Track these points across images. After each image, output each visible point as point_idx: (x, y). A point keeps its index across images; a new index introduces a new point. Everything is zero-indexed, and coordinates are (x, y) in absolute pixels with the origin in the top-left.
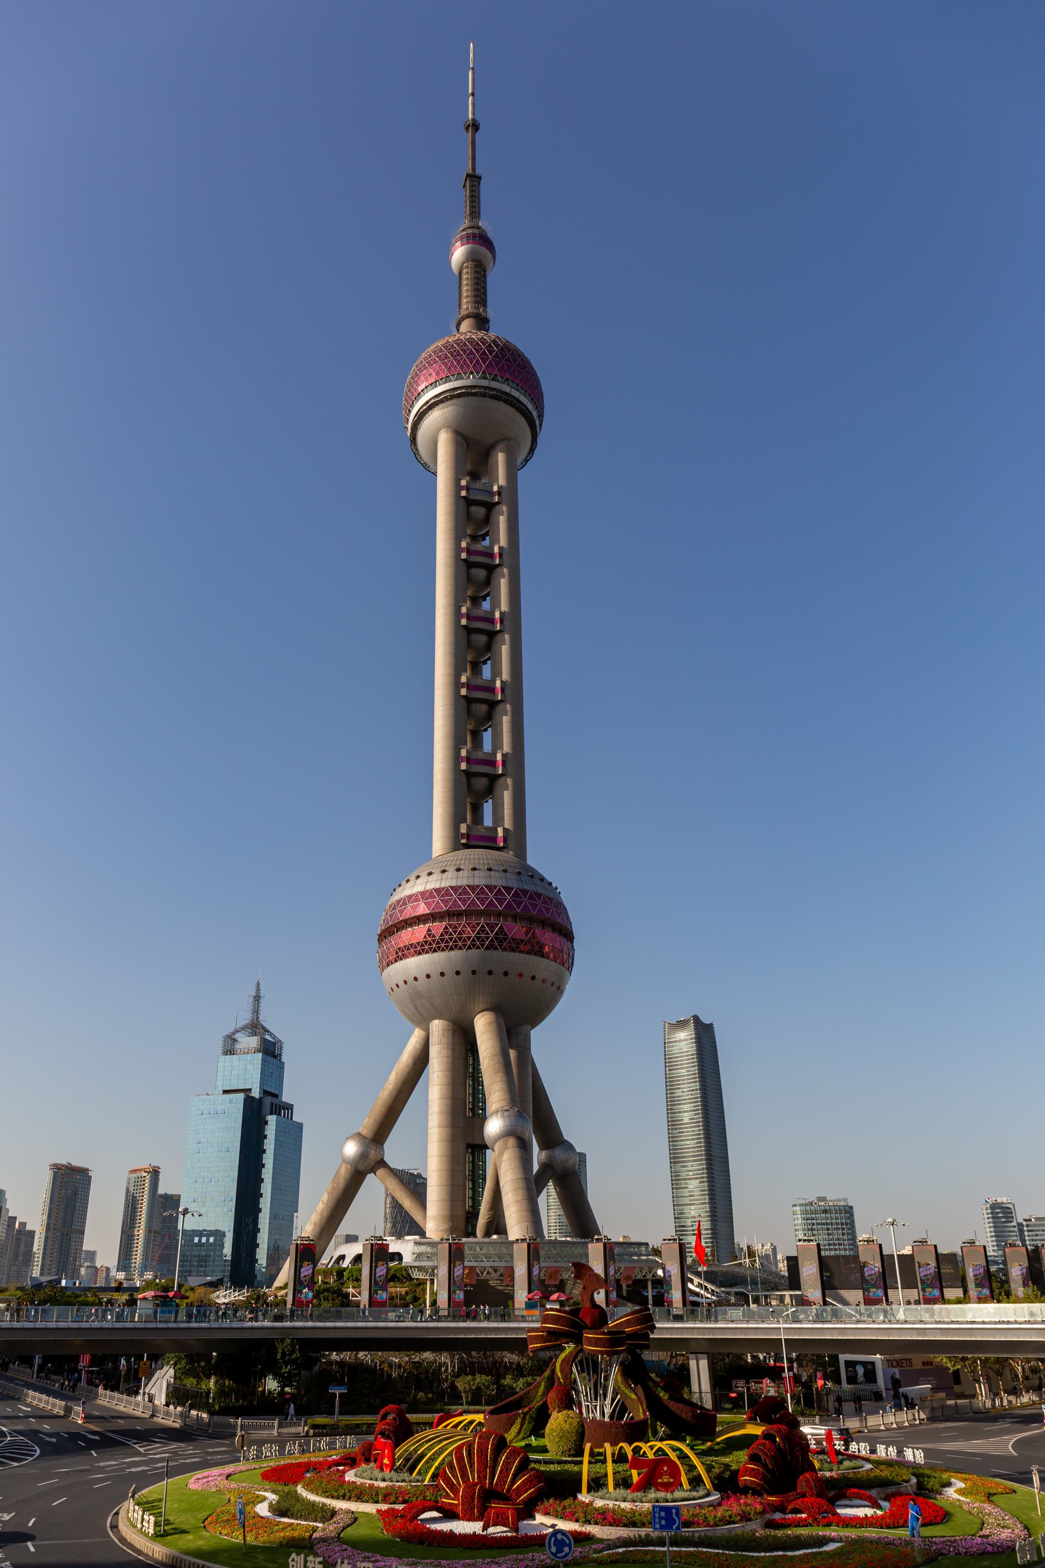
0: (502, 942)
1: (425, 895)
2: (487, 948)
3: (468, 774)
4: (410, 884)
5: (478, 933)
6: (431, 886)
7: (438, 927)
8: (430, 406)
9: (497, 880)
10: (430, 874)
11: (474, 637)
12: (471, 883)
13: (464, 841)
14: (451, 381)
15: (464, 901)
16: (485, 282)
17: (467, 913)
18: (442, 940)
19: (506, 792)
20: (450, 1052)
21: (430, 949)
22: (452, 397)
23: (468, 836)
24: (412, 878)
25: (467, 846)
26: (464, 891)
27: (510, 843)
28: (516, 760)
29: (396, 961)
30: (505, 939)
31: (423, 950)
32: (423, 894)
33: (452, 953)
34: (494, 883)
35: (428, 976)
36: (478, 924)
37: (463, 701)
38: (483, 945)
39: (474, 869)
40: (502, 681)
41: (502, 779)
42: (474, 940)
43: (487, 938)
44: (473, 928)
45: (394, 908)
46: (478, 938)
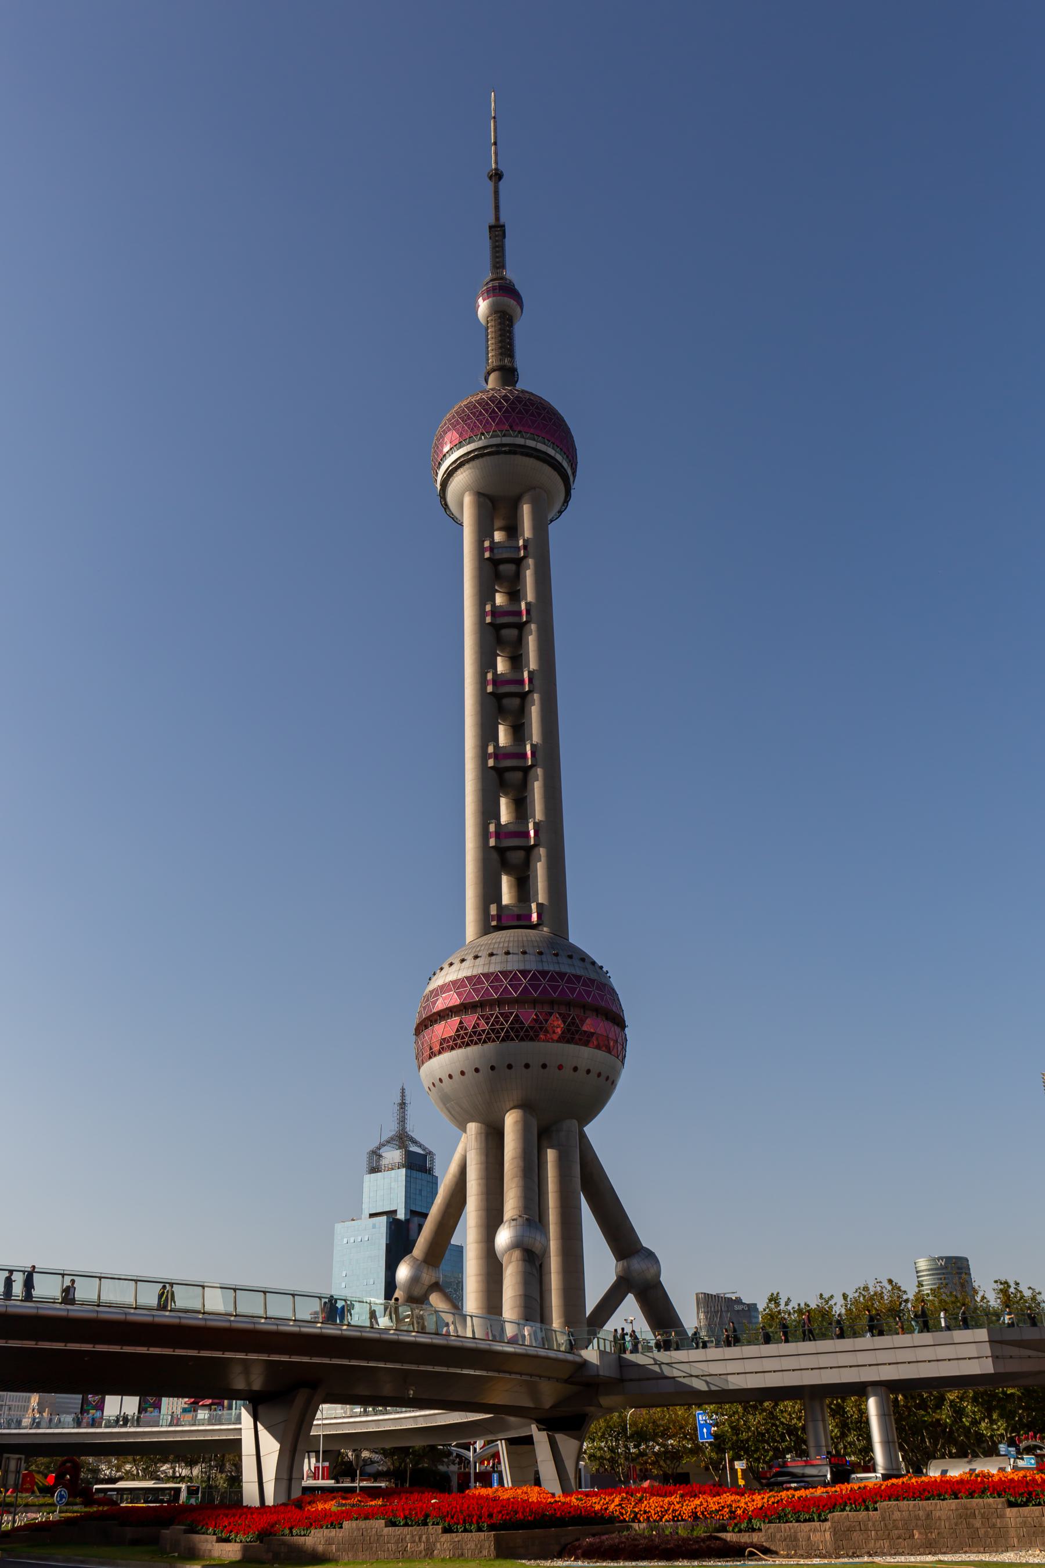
0: (521, 1033)
1: (457, 984)
2: (503, 1040)
3: (500, 850)
4: (444, 972)
5: (493, 1025)
6: (461, 975)
7: (470, 1020)
8: (450, 474)
9: (514, 964)
10: (463, 960)
11: (506, 702)
12: (522, 968)
13: (494, 923)
14: (474, 441)
15: (496, 989)
16: (511, 332)
17: (499, 1002)
18: (475, 1033)
19: (539, 864)
20: (483, 1158)
21: (463, 1043)
22: (468, 461)
23: (499, 917)
24: (446, 966)
25: (499, 928)
26: (497, 978)
27: (546, 918)
28: (553, 828)
29: (430, 1058)
30: (522, 1028)
31: (456, 1045)
32: (454, 982)
33: (485, 1045)
34: (528, 968)
35: (463, 1073)
36: (492, 1015)
37: (493, 773)
38: (498, 1038)
39: (491, 955)
40: (532, 745)
41: (536, 850)
42: (488, 1033)
43: (502, 1029)
44: (487, 1019)
45: (428, 1000)
46: (493, 1030)
